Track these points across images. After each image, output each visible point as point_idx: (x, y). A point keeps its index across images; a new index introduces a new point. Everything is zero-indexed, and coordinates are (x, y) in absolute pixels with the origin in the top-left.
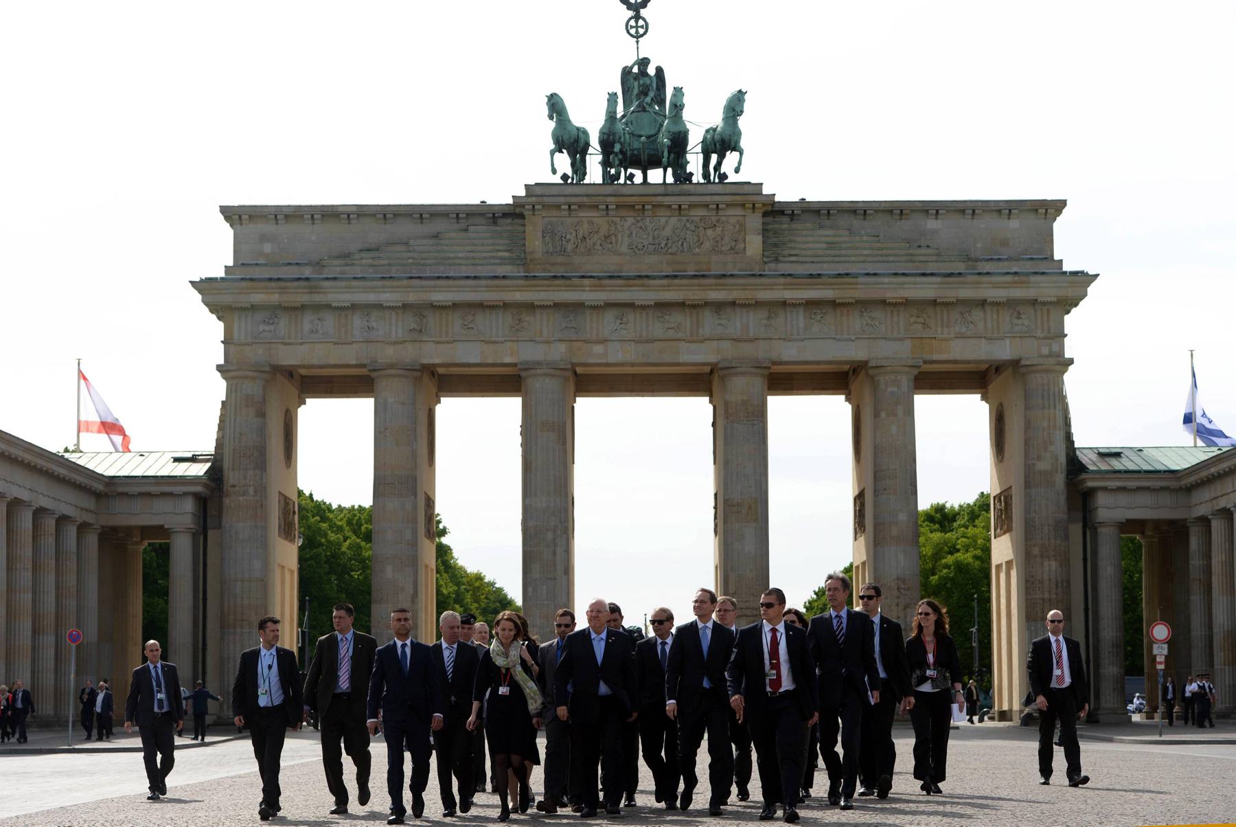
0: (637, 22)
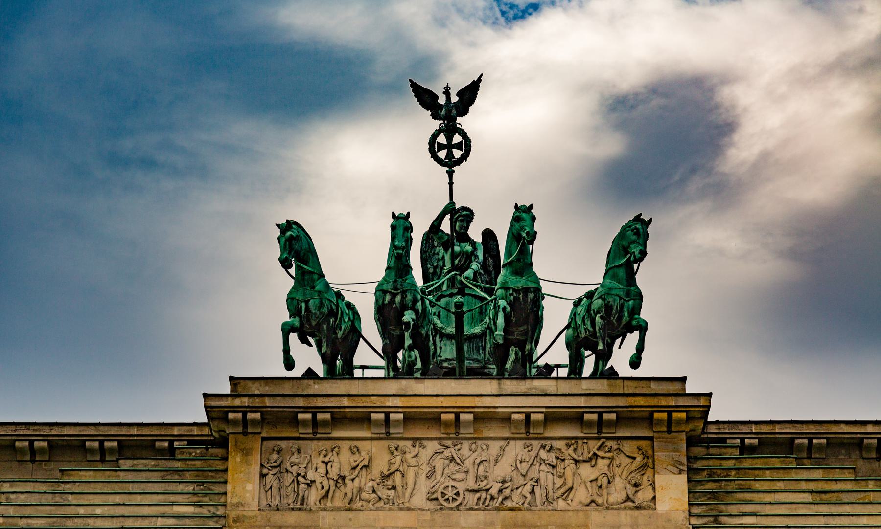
0: (449, 138)
